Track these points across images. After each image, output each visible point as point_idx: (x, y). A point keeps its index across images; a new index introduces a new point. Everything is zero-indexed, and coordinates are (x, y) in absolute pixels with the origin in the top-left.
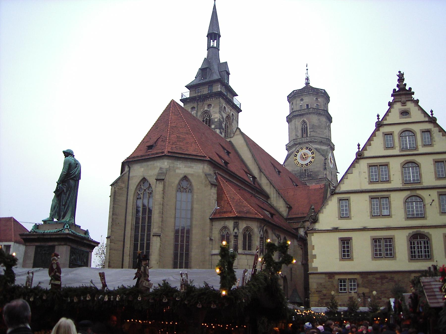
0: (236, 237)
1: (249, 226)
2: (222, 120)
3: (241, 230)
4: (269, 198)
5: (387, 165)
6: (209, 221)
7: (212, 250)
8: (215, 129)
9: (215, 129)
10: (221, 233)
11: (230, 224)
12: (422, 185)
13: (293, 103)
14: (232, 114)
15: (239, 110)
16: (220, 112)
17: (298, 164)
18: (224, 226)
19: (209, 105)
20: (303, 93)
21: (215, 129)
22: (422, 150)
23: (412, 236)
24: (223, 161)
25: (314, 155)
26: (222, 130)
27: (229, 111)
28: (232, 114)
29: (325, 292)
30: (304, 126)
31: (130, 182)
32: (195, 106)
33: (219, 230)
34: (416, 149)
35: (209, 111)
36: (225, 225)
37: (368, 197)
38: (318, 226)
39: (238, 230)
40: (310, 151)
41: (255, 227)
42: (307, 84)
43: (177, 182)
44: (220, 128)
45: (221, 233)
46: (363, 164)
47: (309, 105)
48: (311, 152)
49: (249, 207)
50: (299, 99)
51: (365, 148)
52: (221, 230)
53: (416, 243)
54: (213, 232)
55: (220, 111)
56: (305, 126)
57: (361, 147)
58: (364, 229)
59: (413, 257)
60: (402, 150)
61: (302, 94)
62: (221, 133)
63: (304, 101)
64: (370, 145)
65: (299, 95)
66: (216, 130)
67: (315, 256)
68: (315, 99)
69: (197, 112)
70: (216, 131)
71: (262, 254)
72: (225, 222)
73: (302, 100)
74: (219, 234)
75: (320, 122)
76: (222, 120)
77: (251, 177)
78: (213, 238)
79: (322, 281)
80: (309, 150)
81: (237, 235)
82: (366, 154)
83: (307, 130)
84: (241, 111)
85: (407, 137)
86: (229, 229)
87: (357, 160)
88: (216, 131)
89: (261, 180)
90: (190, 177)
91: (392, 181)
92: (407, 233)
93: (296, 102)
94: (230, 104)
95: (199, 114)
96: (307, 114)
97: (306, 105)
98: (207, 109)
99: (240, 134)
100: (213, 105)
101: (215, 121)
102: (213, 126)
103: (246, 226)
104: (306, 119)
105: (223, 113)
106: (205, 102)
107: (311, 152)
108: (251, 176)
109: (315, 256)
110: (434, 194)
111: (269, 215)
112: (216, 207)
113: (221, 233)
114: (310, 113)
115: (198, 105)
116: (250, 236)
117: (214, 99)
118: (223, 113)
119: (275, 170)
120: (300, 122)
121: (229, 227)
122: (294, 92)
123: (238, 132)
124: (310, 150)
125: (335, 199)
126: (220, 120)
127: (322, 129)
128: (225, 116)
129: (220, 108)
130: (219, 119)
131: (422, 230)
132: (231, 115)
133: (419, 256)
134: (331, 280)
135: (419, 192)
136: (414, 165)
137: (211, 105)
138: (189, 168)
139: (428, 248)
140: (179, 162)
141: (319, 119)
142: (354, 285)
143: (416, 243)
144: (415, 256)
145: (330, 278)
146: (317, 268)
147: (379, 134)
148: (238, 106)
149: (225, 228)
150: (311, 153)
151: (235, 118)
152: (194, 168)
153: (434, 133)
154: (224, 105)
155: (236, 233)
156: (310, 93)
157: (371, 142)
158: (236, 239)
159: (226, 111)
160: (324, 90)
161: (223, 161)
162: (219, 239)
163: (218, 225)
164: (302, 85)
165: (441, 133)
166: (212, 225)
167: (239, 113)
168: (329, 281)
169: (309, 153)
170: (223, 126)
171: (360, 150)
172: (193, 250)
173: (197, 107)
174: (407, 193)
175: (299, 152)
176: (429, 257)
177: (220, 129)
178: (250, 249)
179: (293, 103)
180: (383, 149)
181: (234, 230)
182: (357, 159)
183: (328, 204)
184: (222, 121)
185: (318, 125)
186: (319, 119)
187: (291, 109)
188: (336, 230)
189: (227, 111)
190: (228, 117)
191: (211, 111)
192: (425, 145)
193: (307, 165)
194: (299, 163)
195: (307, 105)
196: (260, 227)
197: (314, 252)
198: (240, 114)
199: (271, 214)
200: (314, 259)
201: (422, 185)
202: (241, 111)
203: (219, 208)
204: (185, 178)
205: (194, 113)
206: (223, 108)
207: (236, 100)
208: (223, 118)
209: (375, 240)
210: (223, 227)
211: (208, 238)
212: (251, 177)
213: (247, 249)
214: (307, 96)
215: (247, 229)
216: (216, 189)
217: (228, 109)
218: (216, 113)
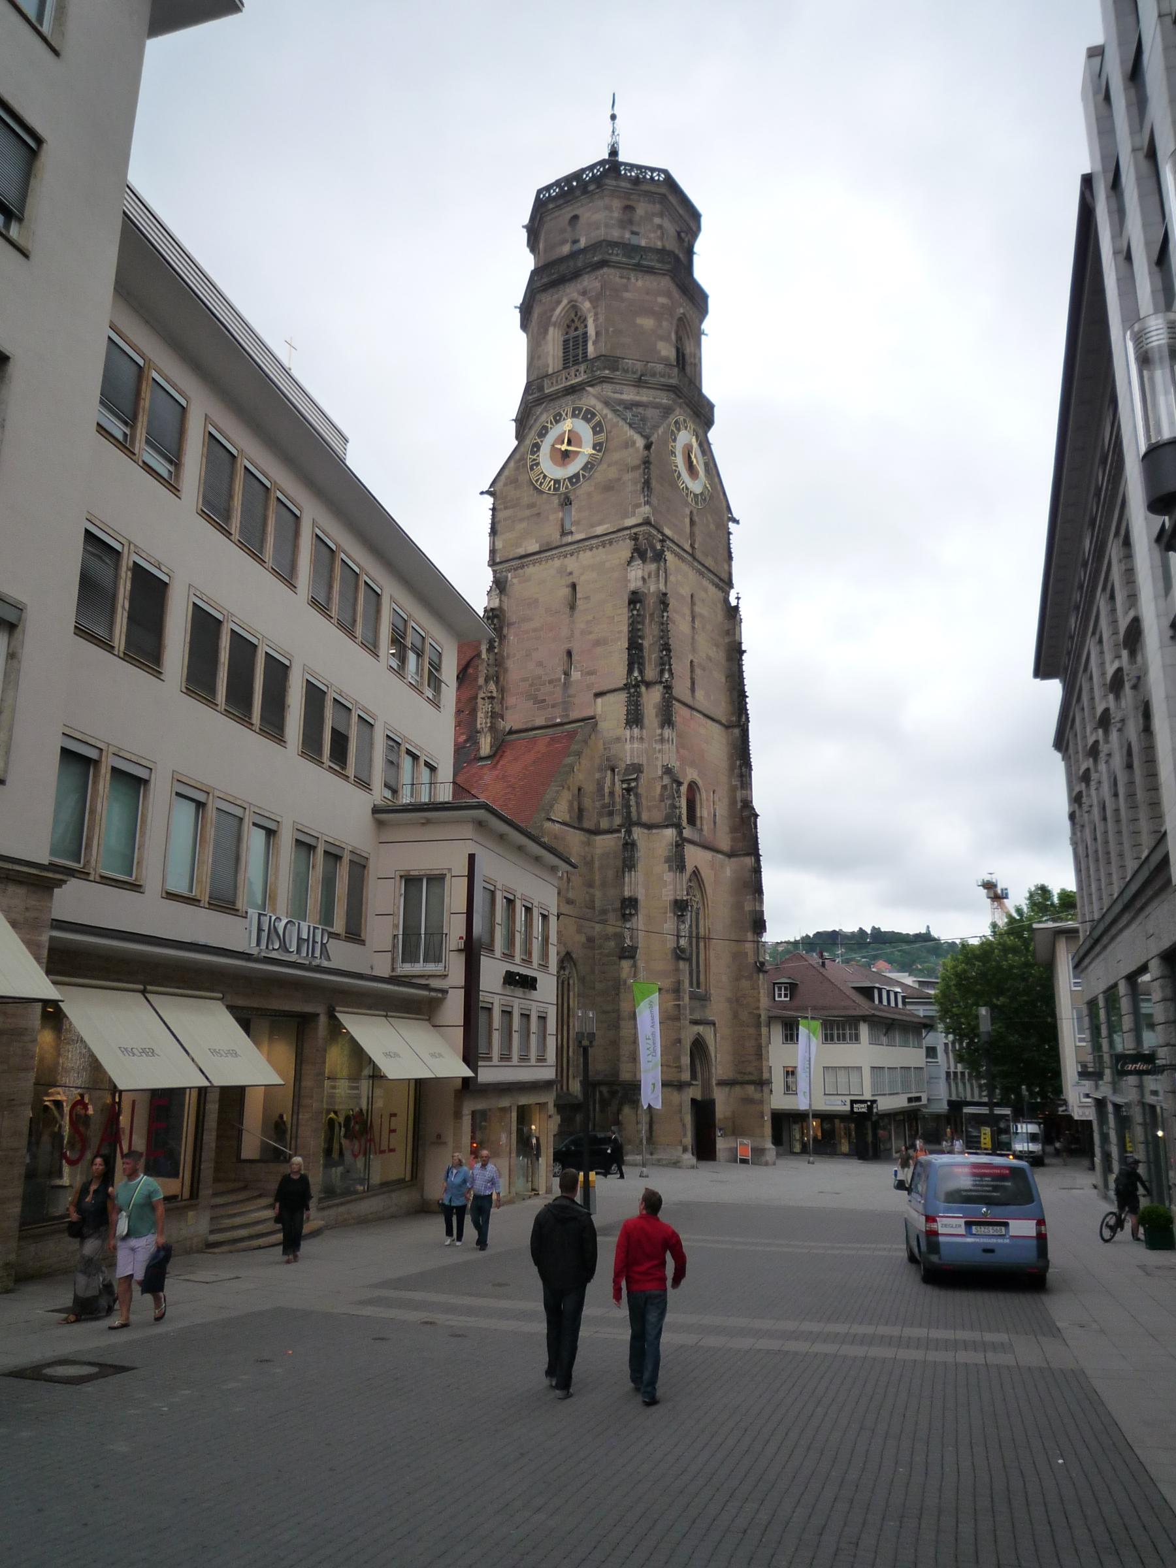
17: (541, 483)
25: (602, 437)
40: (588, 421)
48: (594, 422)
80: (582, 419)
83: (585, 342)
107: (594, 422)
124: (588, 416)
150: (593, 428)
160: (665, 172)
169: (585, 430)
175: (547, 432)
193: (574, 479)
194: (545, 477)
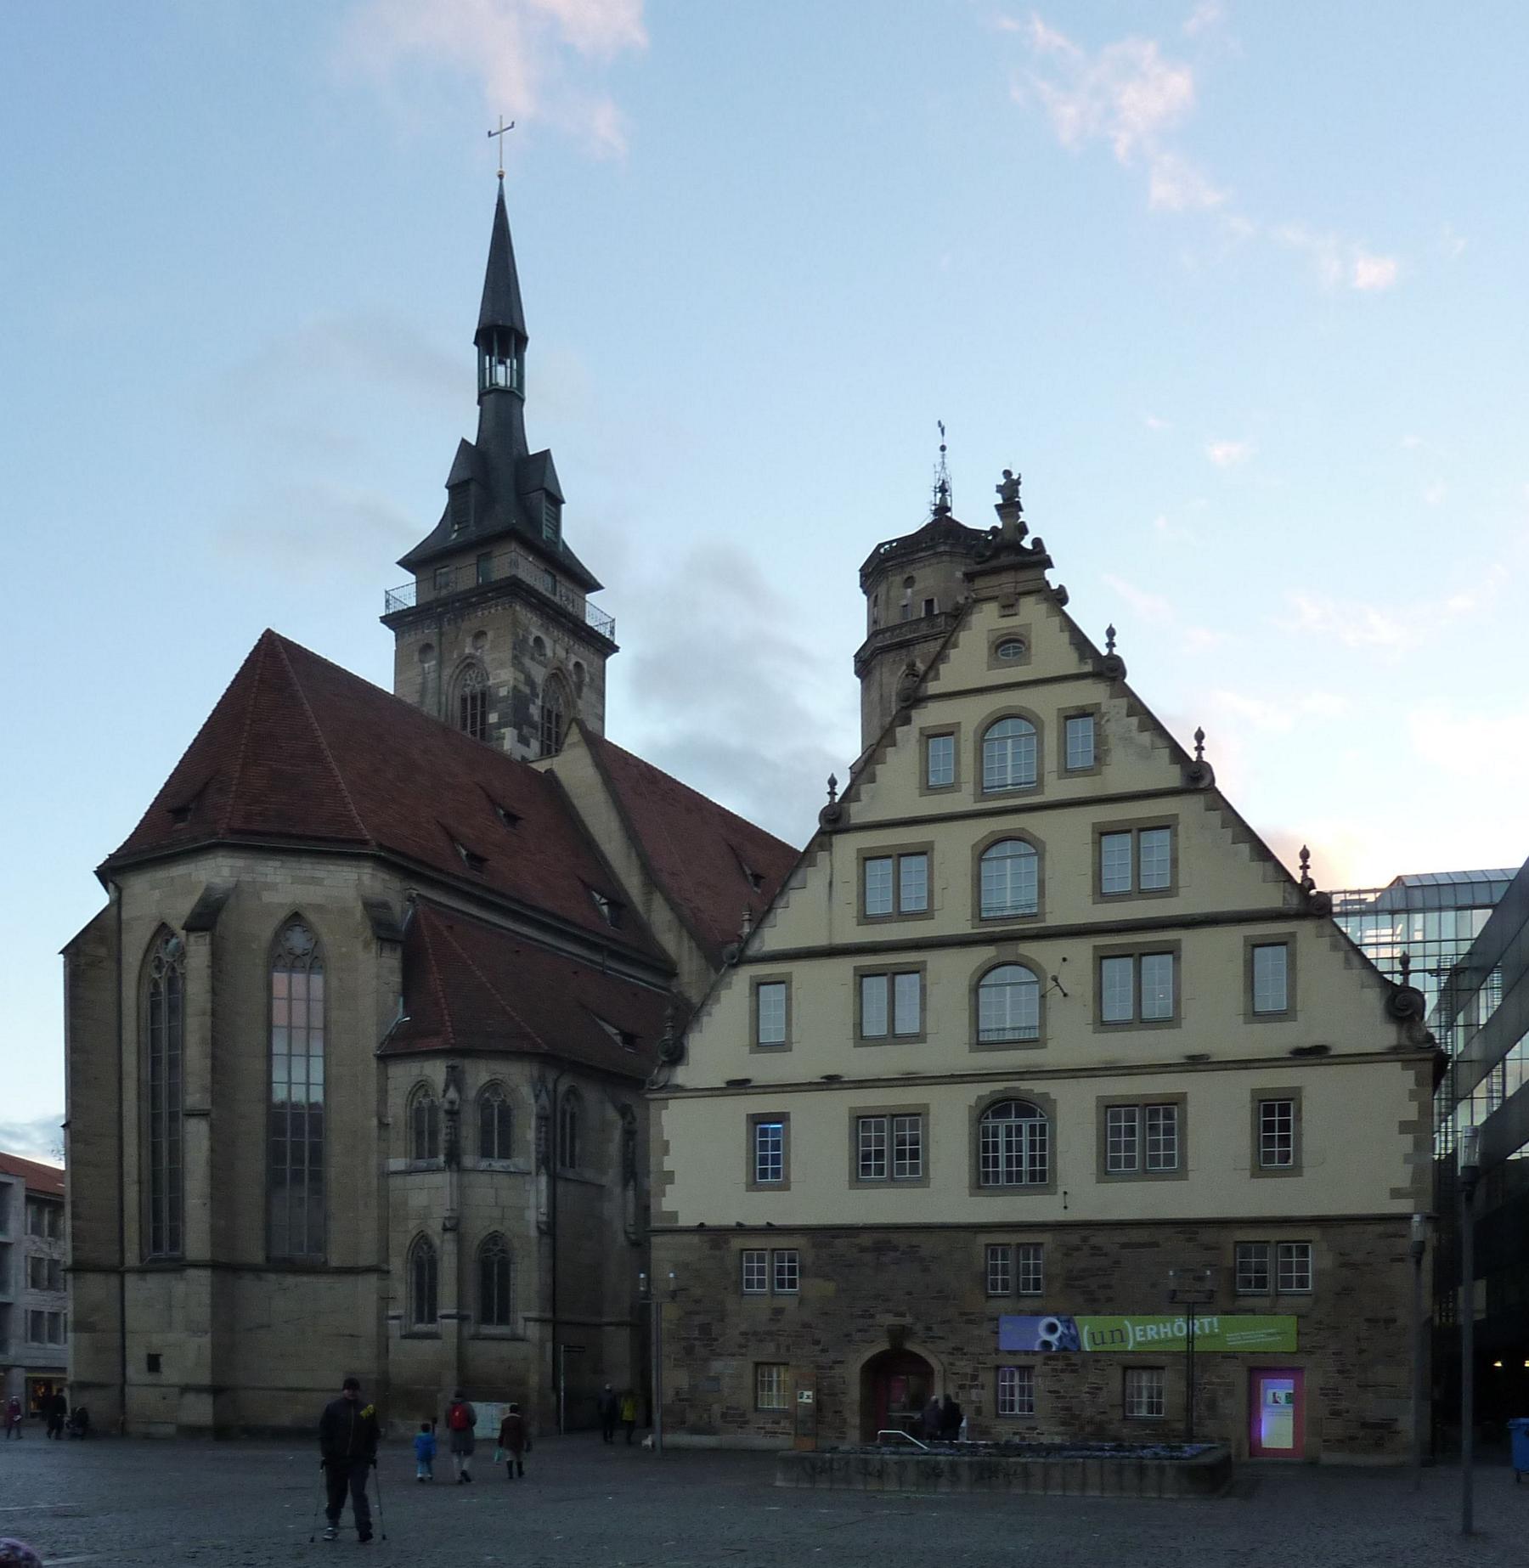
0: (453, 1114)
1: (500, 1077)
2: (527, 690)
3: (472, 1094)
4: (676, 975)
5: (924, 851)
6: (374, 1063)
8: (499, 725)
9: (500, 728)
10: (412, 1101)
11: (436, 1071)
12: (1042, 925)
13: (876, 596)
14: (578, 665)
15: (607, 647)
16: (517, 662)
18: (420, 1079)
19: (480, 635)
20: (918, 551)
21: (499, 725)
22: (1056, 789)
23: (989, 1107)
24: (464, 852)
26: (526, 730)
27: (562, 654)
28: (578, 665)
32: (434, 641)
33: (407, 1093)
34: (1039, 785)
35: (481, 660)
36: (424, 1078)
37: (852, 971)
38: (681, 1076)
39: (459, 1090)
41: (519, 1079)
42: (942, 510)
43: (267, 931)
44: (519, 719)
45: (414, 1104)
46: (847, 847)
47: (936, 601)
50: (898, 580)
51: (851, 794)
52: (413, 1094)
53: (1025, 1130)
55: (515, 657)
57: (840, 790)
58: (832, 1082)
59: (984, 1178)
60: (982, 792)
62: (523, 740)
63: (917, 586)
64: (872, 780)
66: (503, 731)
67: (669, 1177)
69: (440, 664)
70: (504, 733)
71: (543, 1170)
72: (422, 1067)
73: (909, 582)
74: (406, 1105)
76: (527, 690)
77: (604, 904)
78: (390, 1120)
81: (456, 1107)
82: (858, 813)
84: (615, 649)
85: (1010, 741)
87: (825, 839)
88: (504, 733)
89: (649, 910)
90: (312, 917)
91: (936, 913)
92: (973, 1093)
93: (888, 592)
94: (561, 626)
95: (447, 672)
97: (923, 603)
98: (473, 651)
99: (583, 744)
100: (490, 635)
101: (501, 695)
102: (493, 718)
103: (488, 1079)
105: (527, 662)
106: (465, 625)
108: (606, 898)
109: (669, 1177)
110: (1083, 950)
111: (618, 1039)
112: (399, 1017)
115: (441, 634)
116: (506, 1115)
117: (493, 611)
118: (527, 662)
119: (742, 868)
122: (882, 551)
123: (574, 736)
125: (743, 977)
126: (520, 691)
128: (540, 674)
129: (519, 646)
130: (515, 687)
131: (1025, 1085)
132: (571, 667)
133: (1009, 1174)
134: (717, 1253)
135: (1028, 949)
136: (1023, 848)
137: (485, 634)
139: (1043, 1148)
142: (792, 1271)
143: (1025, 1130)
144: (1019, 1173)
145: (716, 1246)
146: (674, 1215)
147: (907, 735)
148: (604, 631)
149: (422, 1086)
151: (587, 679)
153: (1108, 720)
154: (536, 632)
155: (452, 1103)
156: (942, 549)
157: (879, 767)
158: (451, 1123)
159: (545, 655)
161: (464, 852)
162: (406, 1124)
163: (403, 1075)
164: (914, 518)
165: (1134, 721)
166: (388, 1078)
167: (606, 656)
170: (535, 711)
171: (837, 798)
173: (440, 644)
174: (987, 953)
176: (1043, 1179)
177: (517, 726)
178: (506, 1153)
179: (876, 596)
180: (917, 792)
181: (445, 1091)
182: (821, 833)
183: (718, 1000)
184: (526, 696)
187: (873, 621)
188: (739, 1086)
189: (549, 653)
190: (557, 676)
191: (487, 658)
192: (1066, 772)
195: (929, 603)
196: (542, 1080)
197: (668, 1164)
198: (611, 661)
199: (622, 1033)
200: (668, 1187)
201: (1044, 921)
202: (615, 649)
204: (295, 918)
205: (432, 669)
206: (531, 642)
207: (597, 609)
208: (530, 681)
209: (861, 1120)
210: (418, 1082)
211: (375, 1122)
212: (604, 904)
213: (496, 1156)
214: (929, 566)
215: (493, 1086)
216: (399, 954)
217: (556, 647)
218: (502, 665)
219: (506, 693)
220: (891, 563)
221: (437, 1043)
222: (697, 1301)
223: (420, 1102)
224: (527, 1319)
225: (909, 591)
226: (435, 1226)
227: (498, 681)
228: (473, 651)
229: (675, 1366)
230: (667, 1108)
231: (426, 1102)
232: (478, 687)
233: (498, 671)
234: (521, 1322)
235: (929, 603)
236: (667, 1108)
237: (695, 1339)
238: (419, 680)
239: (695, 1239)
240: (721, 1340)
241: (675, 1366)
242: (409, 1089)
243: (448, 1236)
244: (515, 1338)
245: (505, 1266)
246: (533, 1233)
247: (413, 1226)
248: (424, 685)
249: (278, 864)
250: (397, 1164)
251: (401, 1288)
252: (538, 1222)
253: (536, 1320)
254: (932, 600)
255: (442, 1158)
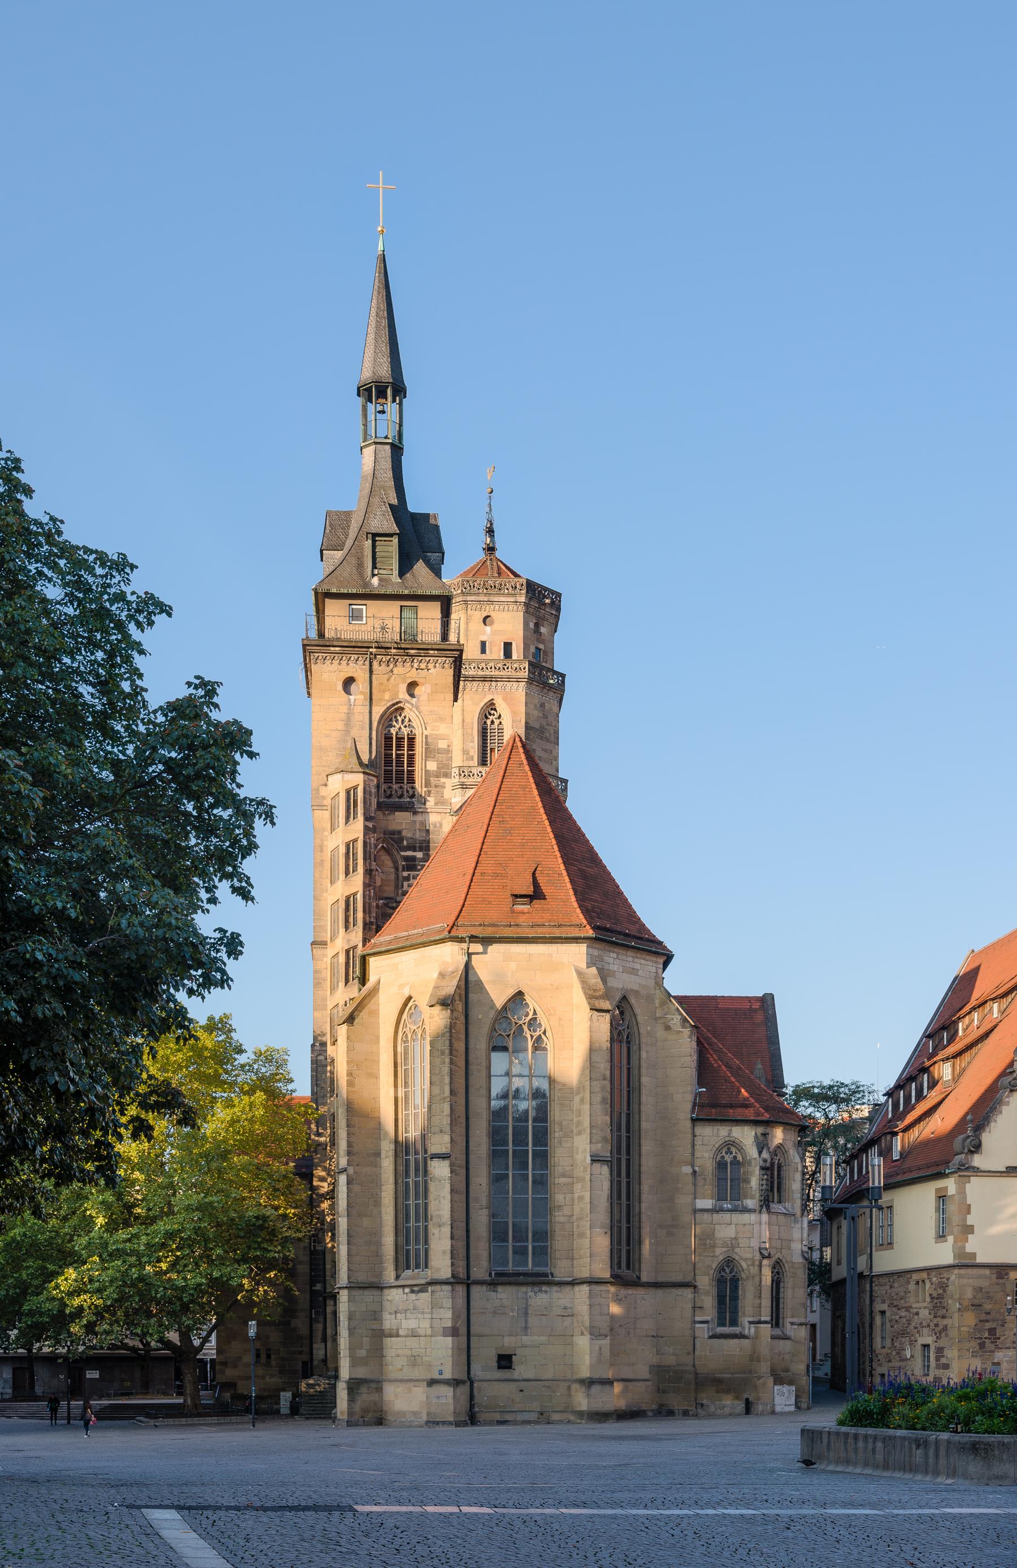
6: (688, 1124)
7: (695, 1199)
29: (988, 1307)
30: (492, 722)
31: (471, 996)
49: (733, 1083)
52: (719, 1150)
54: (697, 1154)
56: (497, 722)
61: (492, 598)
63: (496, 626)
65: (481, 598)
66: (443, 780)
68: (532, 625)
70: (445, 783)
72: (730, 1130)
75: (545, 717)
79: (984, 1283)
86: (740, 1149)
88: (445, 783)
96: (509, 679)
104: (504, 699)
113: (719, 1157)
114: (518, 680)
120: (482, 704)
121: (742, 1144)
127: (548, 740)
134: (1001, 1281)
138: (631, 974)
140: (612, 955)
141: (542, 705)
145: (1000, 1276)
146: (973, 1255)
149: (730, 1145)
152: (640, 972)
155: (765, 1161)
163: (712, 1135)
168: (997, 1284)
172: (644, 1197)
181: (760, 1153)
185: (537, 726)
186: (542, 705)
195: (508, 647)
200: (970, 1236)
203: (704, 1090)
211: (687, 1170)
219: (446, 747)
220: (473, 598)
221: (750, 1114)
222: (988, 1313)
223: (723, 1157)
224: (792, 1324)
225: (488, 629)
226: (746, 1254)
227: (436, 732)
228: (408, 697)
229: (972, 1356)
230: (969, 1182)
231: (728, 1158)
232: (405, 731)
233: (437, 724)
234: (788, 1326)
235: (508, 647)
236: (969, 1182)
237: (986, 1338)
238: (344, 709)
239: (987, 1272)
240: (1002, 1338)
241: (972, 1356)
242: (717, 1146)
243: (765, 1262)
244: (742, 1336)
245: (735, 1282)
246: (798, 1259)
247: (720, 1253)
248: (349, 715)
249: (615, 955)
250: (707, 1203)
251: (709, 1302)
252: (802, 1252)
253: (801, 1324)
254: (511, 644)
255: (751, 1203)
